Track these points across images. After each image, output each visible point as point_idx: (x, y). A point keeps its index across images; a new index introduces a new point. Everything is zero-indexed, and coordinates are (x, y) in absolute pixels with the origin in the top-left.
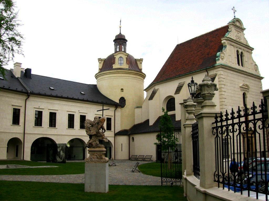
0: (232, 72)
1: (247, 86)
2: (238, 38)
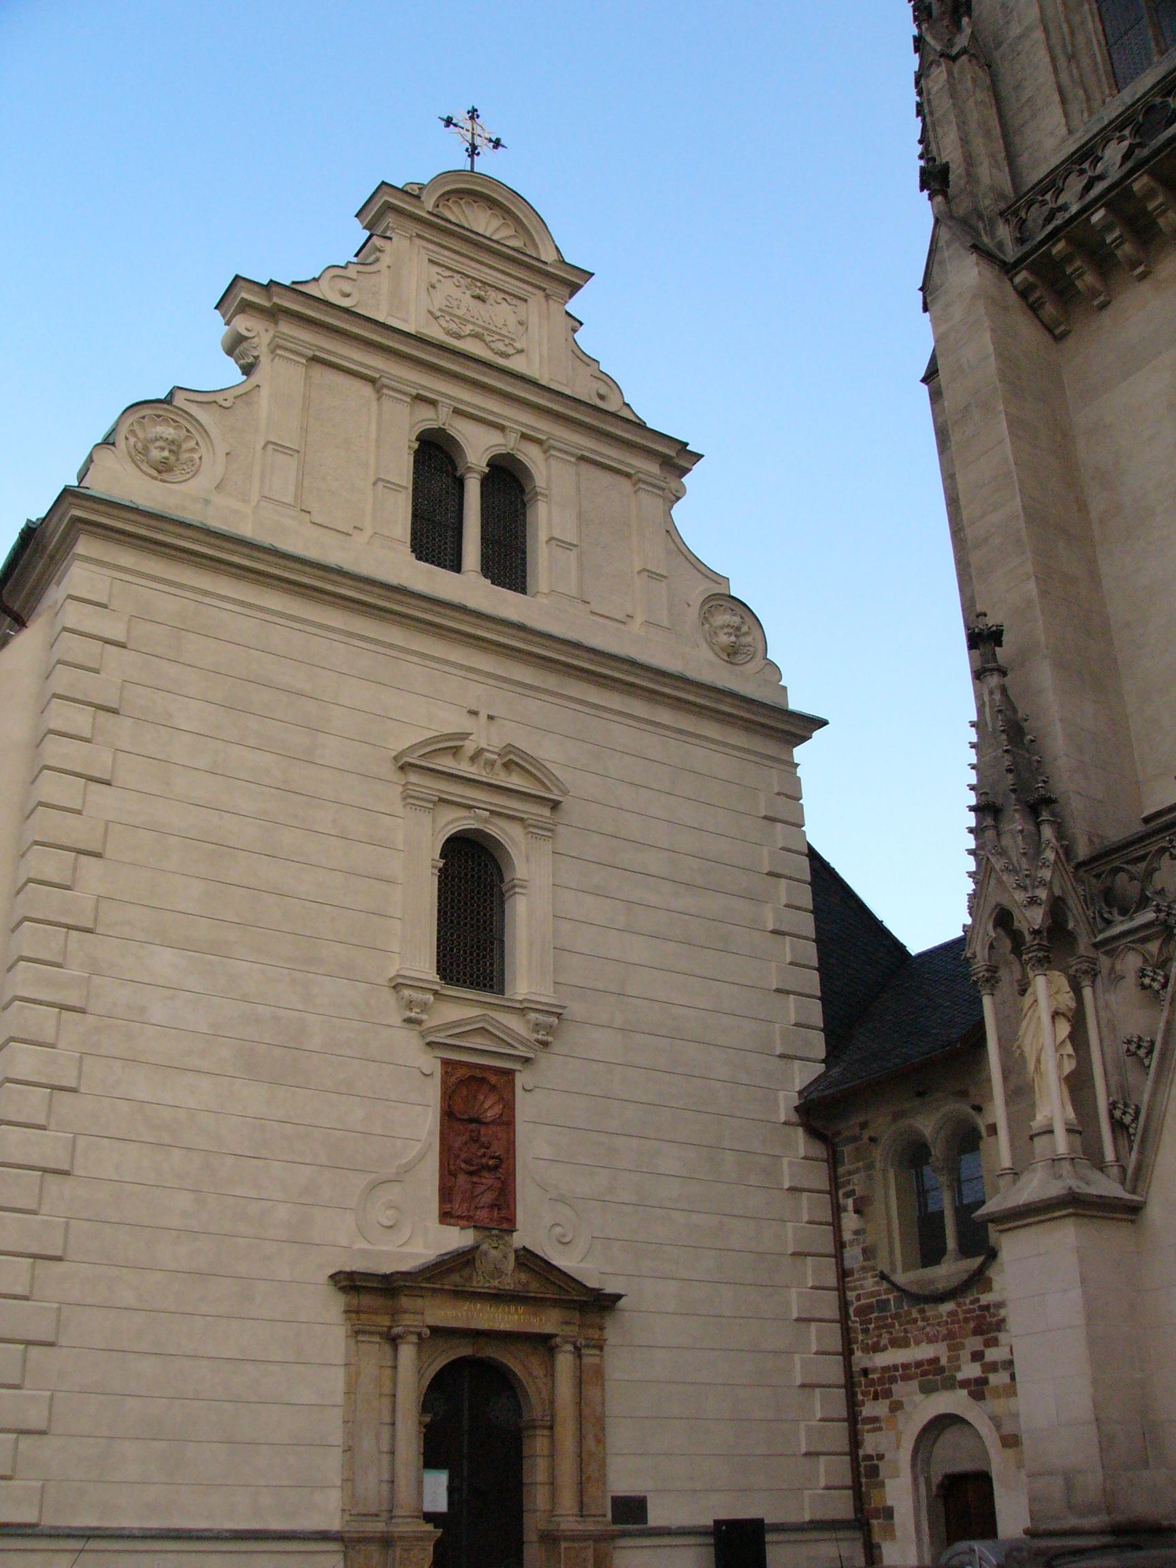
0: (274, 600)
1: (513, 760)
2: (476, 336)
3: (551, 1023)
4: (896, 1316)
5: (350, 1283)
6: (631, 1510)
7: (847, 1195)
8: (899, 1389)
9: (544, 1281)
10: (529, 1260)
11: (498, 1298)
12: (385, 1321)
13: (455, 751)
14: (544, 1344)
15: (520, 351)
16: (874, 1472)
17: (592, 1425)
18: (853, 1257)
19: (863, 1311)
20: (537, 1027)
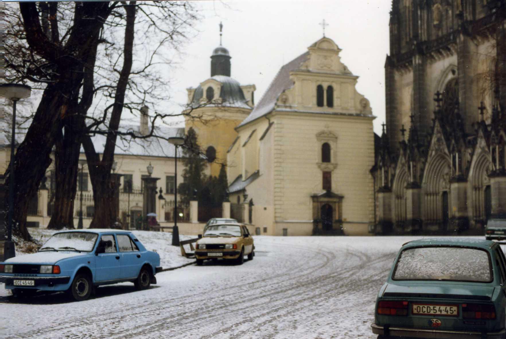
3: (336, 166)
14: (335, 202)
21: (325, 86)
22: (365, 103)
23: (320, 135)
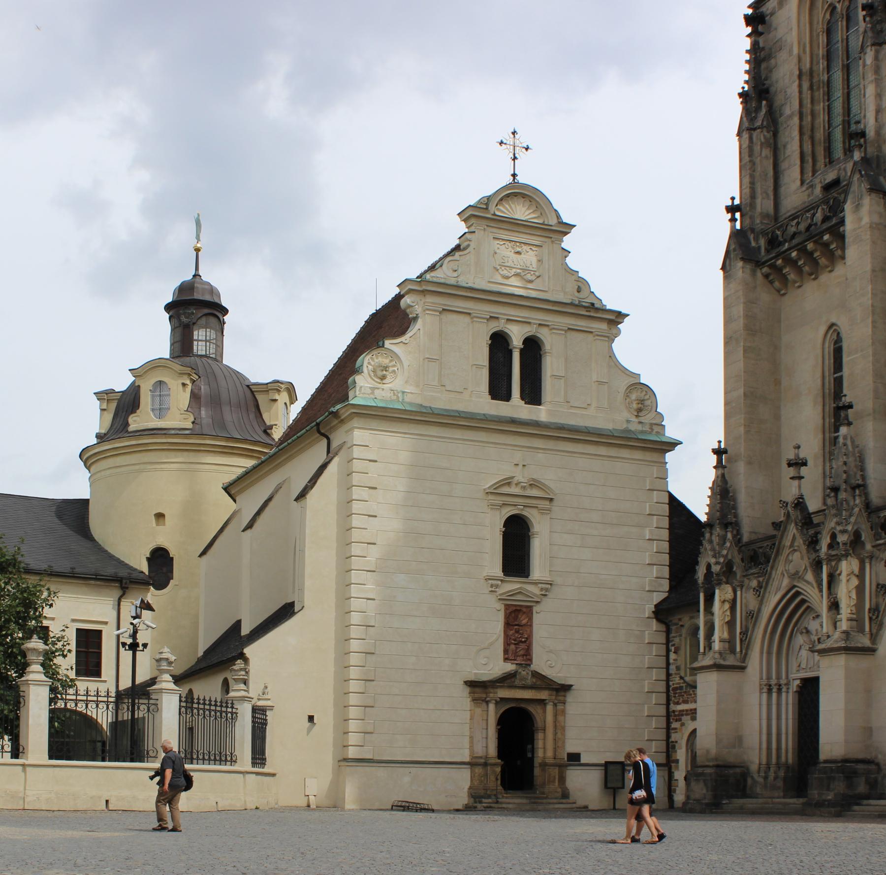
2: (517, 275)
3: (548, 587)
4: (685, 692)
5: (472, 684)
6: (574, 758)
7: (673, 645)
8: (684, 718)
9: (542, 682)
10: (536, 674)
11: (524, 687)
12: (484, 696)
13: (509, 484)
14: (542, 702)
15: (538, 277)
16: (674, 747)
17: (559, 728)
18: (672, 669)
19: (675, 689)
20: (542, 589)
21: (517, 336)
22: (641, 397)
23: (498, 491)
